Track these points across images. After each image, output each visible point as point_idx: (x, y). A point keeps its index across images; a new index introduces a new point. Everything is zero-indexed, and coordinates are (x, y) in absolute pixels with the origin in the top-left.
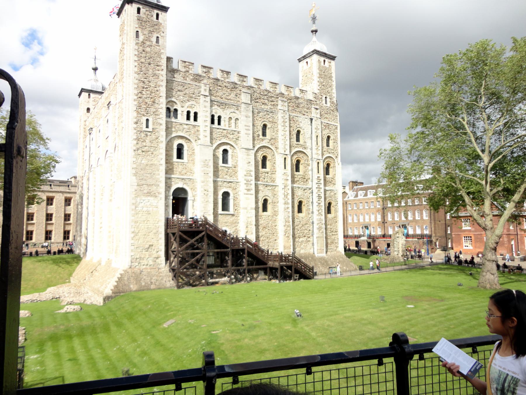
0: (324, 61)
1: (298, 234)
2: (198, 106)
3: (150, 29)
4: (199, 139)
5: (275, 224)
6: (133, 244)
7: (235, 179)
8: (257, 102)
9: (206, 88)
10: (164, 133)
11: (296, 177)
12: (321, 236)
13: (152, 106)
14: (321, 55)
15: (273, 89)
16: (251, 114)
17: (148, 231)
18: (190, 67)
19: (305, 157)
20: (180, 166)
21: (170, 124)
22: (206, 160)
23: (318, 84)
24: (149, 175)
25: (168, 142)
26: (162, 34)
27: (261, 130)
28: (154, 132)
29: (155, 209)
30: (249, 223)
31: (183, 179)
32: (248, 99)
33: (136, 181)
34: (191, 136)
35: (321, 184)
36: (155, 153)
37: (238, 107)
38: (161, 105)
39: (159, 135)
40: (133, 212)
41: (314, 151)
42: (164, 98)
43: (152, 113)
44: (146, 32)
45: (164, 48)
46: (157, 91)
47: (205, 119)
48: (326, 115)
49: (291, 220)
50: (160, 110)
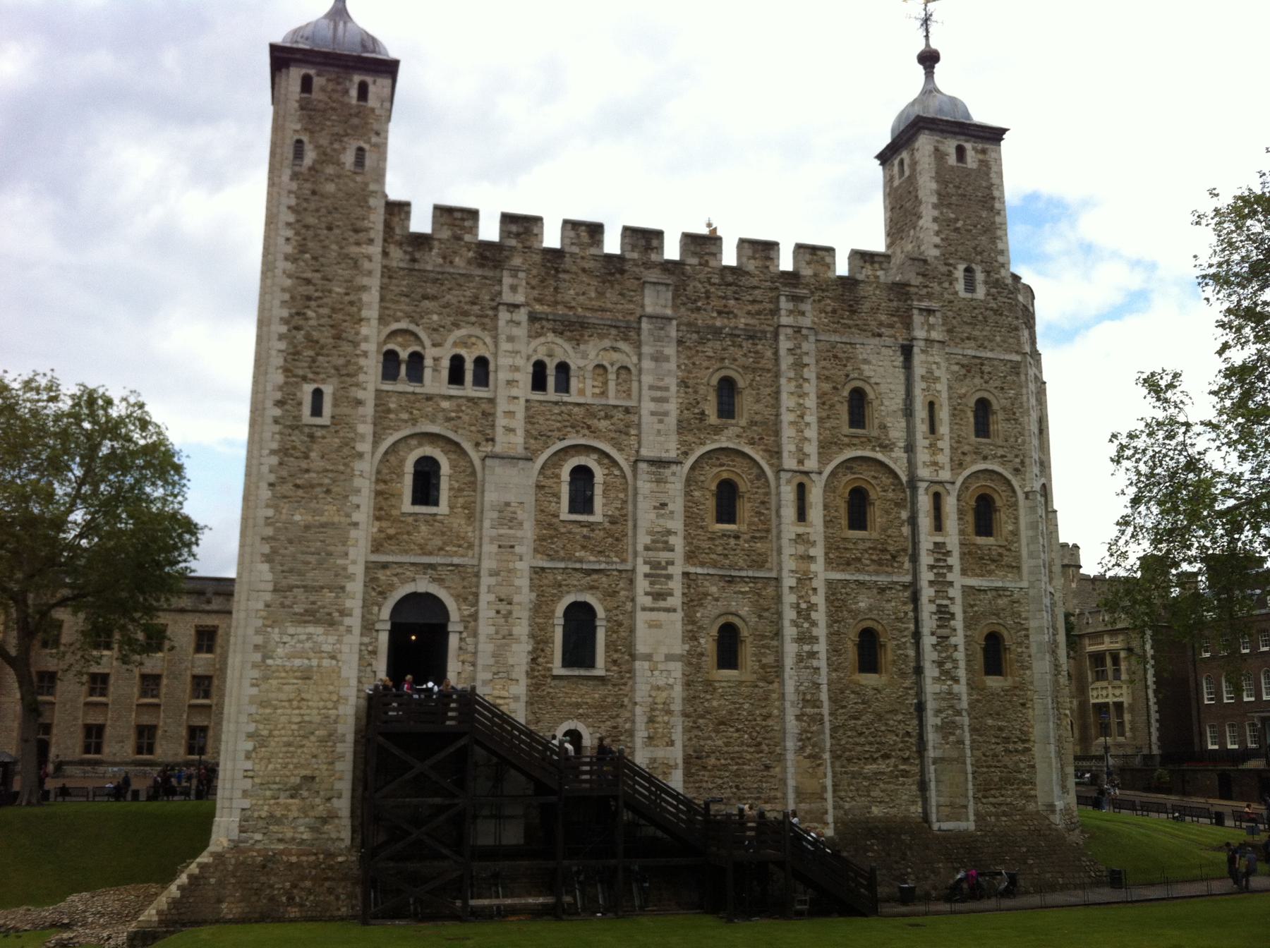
0: (961, 151)
1: (859, 748)
2: (488, 340)
3: (336, 130)
4: (487, 440)
5: (764, 711)
6: (250, 774)
7: (615, 559)
8: (699, 309)
9: (515, 281)
10: (366, 429)
11: (851, 546)
12: (955, 754)
13: (334, 352)
14: (942, 131)
15: (759, 263)
16: (671, 350)
17: (302, 732)
18: (467, 224)
19: (886, 480)
20: (423, 528)
21: (394, 399)
22: (508, 504)
23: (936, 227)
24: (312, 559)
25: (386, 453)
26: (374, 139)
27: (712, 398)
28: (338, 428)
29: (326, 662)
30: (660, 706)
31: (432, 566)
32: (662, 302)
33: (269, 577)
34: (460, 431)
35: (950, 568)
36: (335, 489)
37: (628, 330)
38: (364, 346)
39: (352, 435)
40: (256, 673)
41: (922, 456)
42: (374, 323)
43: (333, 371)
44: (324, 142)
45: (380, 176)
46: (351, 303)
47: (510, 376)
48: (968, 329)
49: (824, 696)
50: (362, 361)
